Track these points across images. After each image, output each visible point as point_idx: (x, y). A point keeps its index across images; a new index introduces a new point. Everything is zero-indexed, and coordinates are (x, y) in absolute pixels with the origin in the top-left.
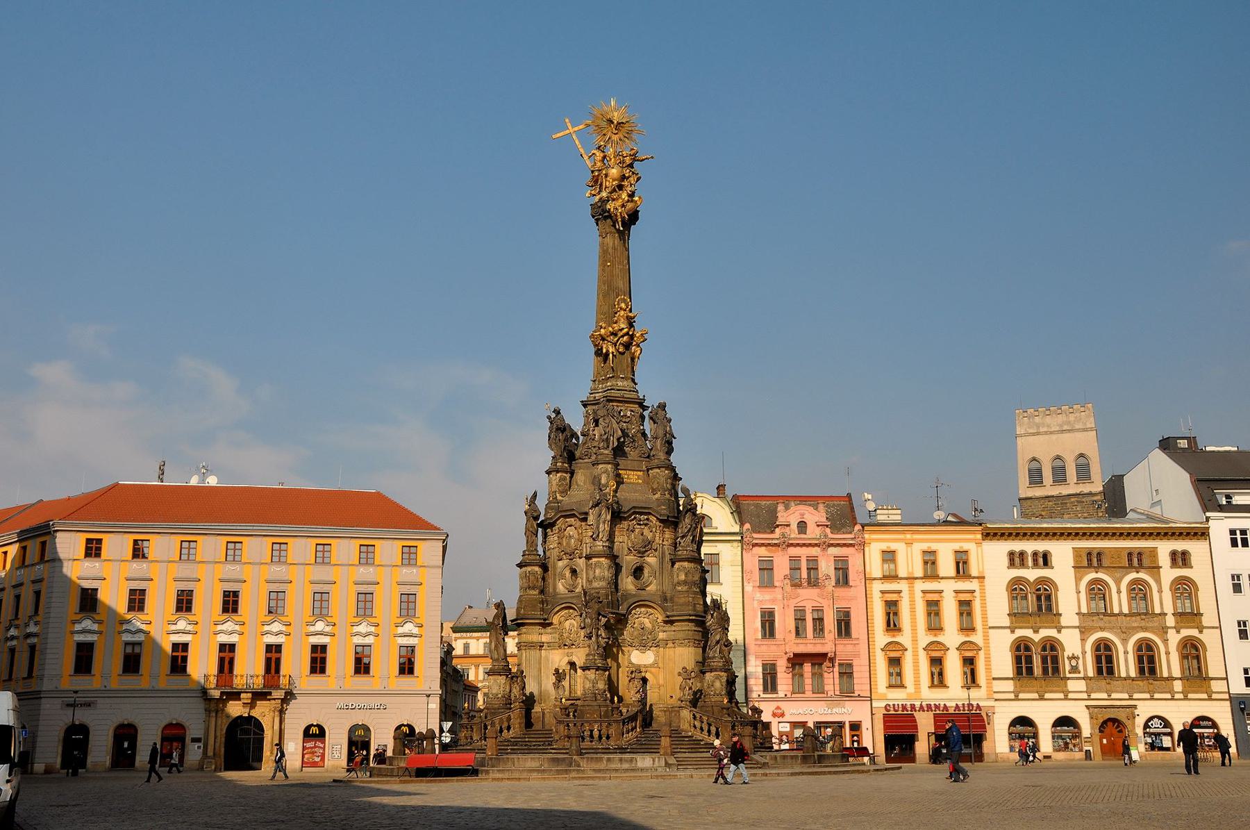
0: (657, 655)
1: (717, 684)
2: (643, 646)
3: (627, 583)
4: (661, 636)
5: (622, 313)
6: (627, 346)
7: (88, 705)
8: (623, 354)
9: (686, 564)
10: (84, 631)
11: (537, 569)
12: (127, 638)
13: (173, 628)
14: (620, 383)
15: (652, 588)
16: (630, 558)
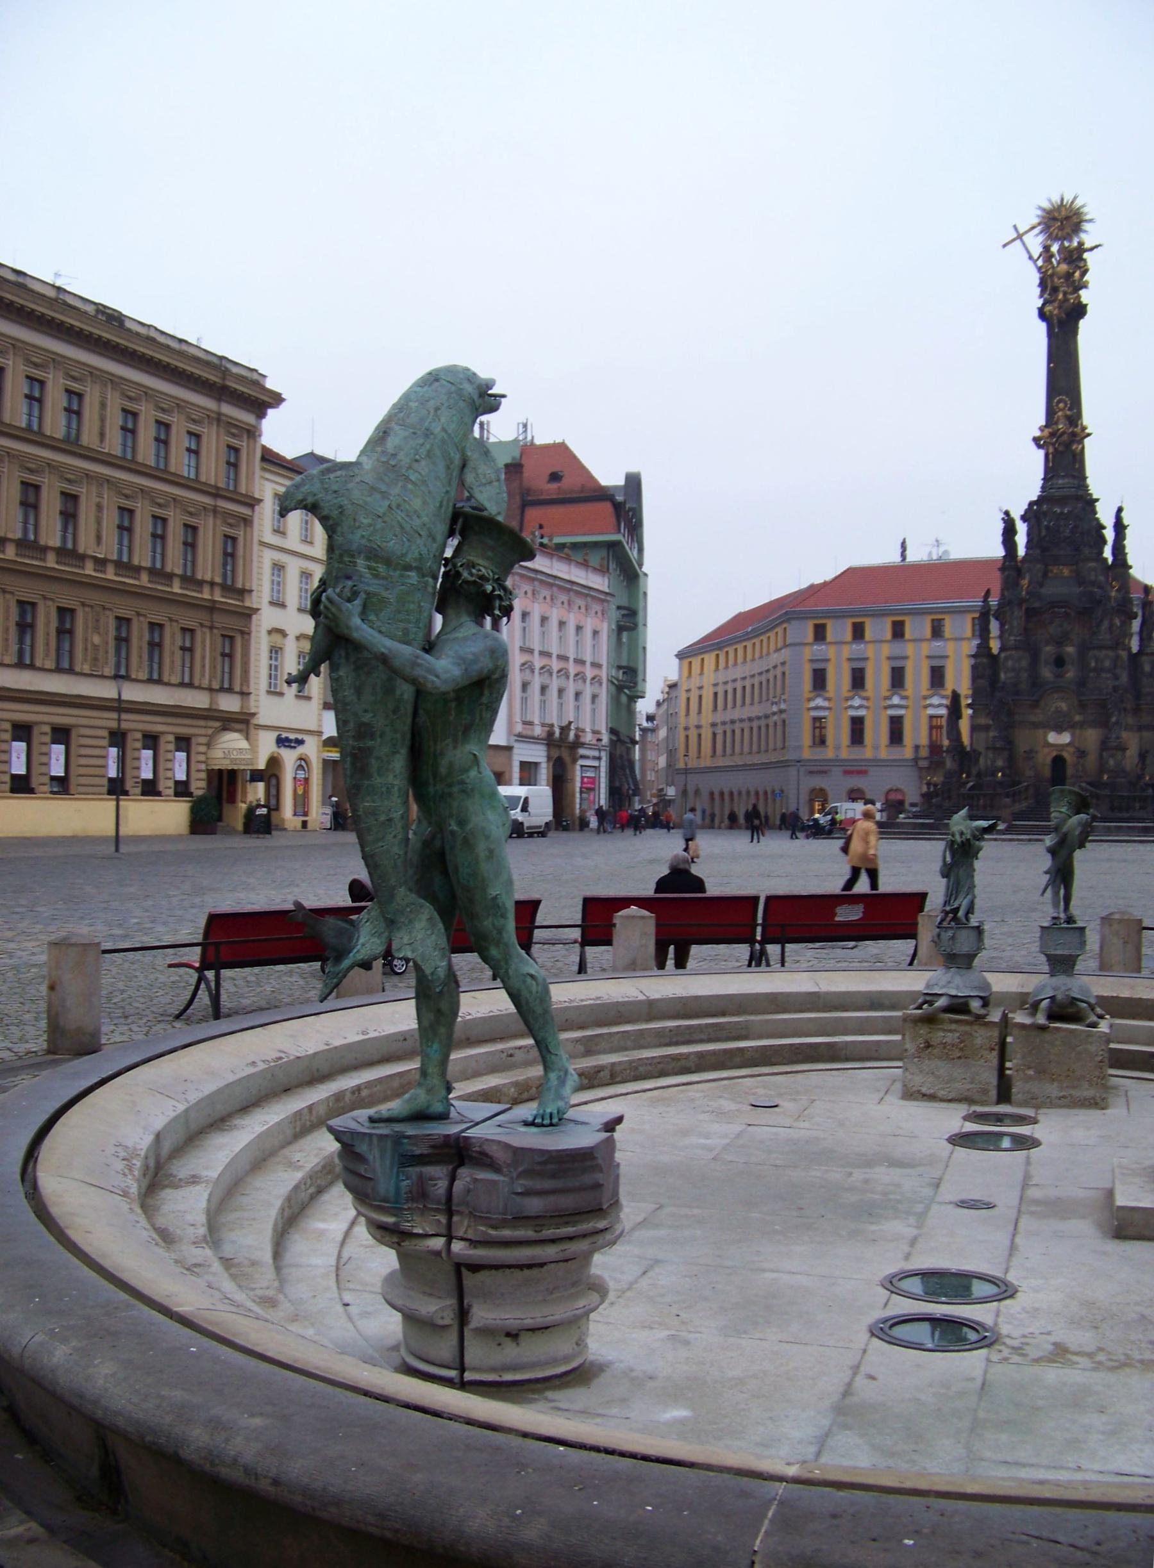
0: (1073, 736)
1: (1112, 762)
2: (1059, 729)
3: (1047, 673)
4: (1078, 718)
5: (1060, 413)
6: (1068, 445)
7: (825, 772)
8: (1062, 453)
9: (1096, 652)
10: (817, 708)
11: (985, 660)
12: (852, 713)
13: (889, 702)
14: (1060, 482)
15: (1070, 675)
16: (1048, 648)
